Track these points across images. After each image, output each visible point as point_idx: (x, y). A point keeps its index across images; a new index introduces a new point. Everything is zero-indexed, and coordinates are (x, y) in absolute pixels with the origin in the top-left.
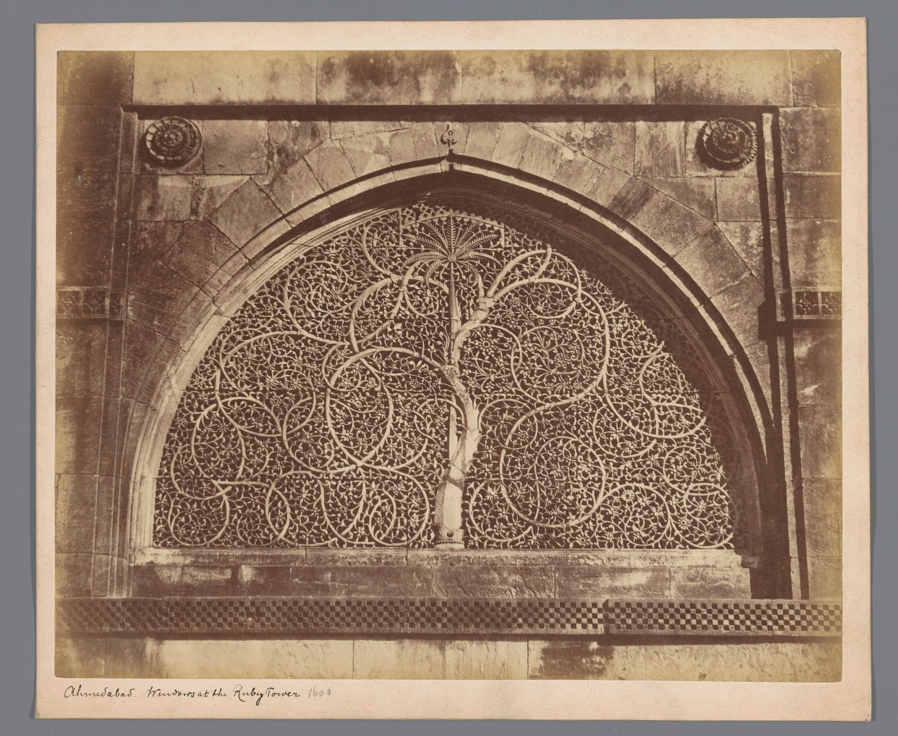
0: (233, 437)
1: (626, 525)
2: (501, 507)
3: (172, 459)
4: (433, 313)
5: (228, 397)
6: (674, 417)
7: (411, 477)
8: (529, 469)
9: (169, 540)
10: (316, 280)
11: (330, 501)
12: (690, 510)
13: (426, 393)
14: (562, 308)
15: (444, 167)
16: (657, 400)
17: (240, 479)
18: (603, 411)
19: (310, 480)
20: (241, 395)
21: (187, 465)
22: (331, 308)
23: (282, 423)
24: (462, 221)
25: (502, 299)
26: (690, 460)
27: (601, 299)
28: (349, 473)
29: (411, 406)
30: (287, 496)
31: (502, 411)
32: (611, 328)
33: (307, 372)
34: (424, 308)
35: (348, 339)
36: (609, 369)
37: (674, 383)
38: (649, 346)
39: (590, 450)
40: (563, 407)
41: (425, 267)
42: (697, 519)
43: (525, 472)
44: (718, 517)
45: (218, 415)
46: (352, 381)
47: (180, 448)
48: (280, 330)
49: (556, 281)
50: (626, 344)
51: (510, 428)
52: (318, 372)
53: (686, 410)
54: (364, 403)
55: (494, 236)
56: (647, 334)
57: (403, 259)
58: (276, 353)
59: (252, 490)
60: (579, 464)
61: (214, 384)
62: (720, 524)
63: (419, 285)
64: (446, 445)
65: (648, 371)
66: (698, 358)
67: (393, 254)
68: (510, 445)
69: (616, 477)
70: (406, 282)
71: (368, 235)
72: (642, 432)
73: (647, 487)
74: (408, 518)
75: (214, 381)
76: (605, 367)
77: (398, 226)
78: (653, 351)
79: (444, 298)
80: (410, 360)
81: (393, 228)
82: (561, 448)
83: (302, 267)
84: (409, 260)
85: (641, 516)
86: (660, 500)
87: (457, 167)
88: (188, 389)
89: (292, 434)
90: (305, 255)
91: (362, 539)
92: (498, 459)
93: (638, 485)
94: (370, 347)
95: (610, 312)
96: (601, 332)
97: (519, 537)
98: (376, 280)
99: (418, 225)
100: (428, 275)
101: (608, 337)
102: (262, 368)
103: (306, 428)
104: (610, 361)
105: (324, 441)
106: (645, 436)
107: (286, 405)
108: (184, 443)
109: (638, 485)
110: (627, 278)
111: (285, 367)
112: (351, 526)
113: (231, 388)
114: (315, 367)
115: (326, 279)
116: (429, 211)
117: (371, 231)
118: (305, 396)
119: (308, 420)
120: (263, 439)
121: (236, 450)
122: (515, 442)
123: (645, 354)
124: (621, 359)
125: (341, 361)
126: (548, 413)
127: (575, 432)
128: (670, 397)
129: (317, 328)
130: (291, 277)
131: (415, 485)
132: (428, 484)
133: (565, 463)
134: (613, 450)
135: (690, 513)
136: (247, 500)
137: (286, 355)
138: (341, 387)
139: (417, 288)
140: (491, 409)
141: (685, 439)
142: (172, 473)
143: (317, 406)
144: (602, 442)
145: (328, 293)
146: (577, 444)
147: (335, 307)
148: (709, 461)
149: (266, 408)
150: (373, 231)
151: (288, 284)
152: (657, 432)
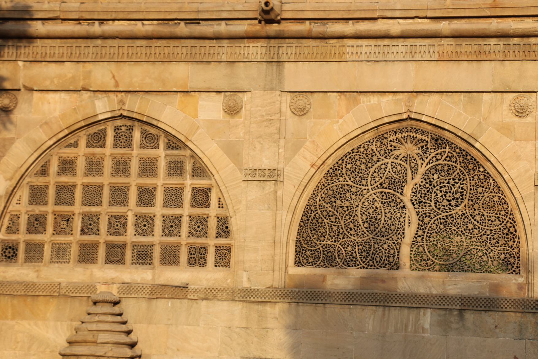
3: (301, 232)
4: (400, 176)
6: (493, 220)
7: (390, 242)
9: (301, 264)
10: (356, 161)
11: (360, 251)
13: (397, 208)
14: (452, 174)
15: (405, 116)
16: (487, 213)
17: (326, 241)
18: (466, 217)
19: (352, 242)
20: (327, 208)
22: (361, 173)
23: (342, 219)
24: (413, 137)
25: (428, 170)
27: (467, 170)
28: (367, 240)
29: (391, 213)
30: (344, 248)
31: (426, 216)
32: (470, 183)
34: (397, 173)
35: (367, 186)
36: (469, 200)
37: (494, 206)
38: (485, 191)
39: (460, 233)
40: (450, 215)
41: (398, 156)
42: (501, 262)
44: (509, 261)
47: (304, 229)
49: (450, 163)
50: (476, 190)
51: (429, 223)
52: (356, 199)
53: (499, 217)
54: (373, 212)
55: (426, 143)
57: (389, 153)
59: (331, 246)
62: (510, 264)
63: (395, 164)
64: (404, 230)
66: (505, 196)
67: (385, 151)
68: (429, 230)
70: (390, 163)
71: (376, 142)
72: (480, 226)
74: (389, 258)
75: (316, 202)
76: (467, 199)
78: (487, 193)
79: (405, 169)
82: (448, 232)
83: (350, 156)
84: (392, 153)
89: (346, 224)
90: (352, 150)
91: (371, 266)
92: (423, 235)
93: (478, 247)
94: (375, 189)
95: (471, 176)
97: (431, 267)
98: (378, 161)
100: (399, 159)
102: (335, 197)
103: (351, 222)
104: (469, 197)
105: (358, 227)
106: (482, 228)
107: (344, 212)
108: (306, 227)
109: (478, 247)
110: (478, 162)
111: (343, 197)
112: (367, 261)
114: (355, 198)
115: (359, 161)
116: (400, 132)
118: (351, 209)
119: (352, 218)
120: (335, 226)
121: (325, 230)
122: (430, 229)
123: (483, 194)
124: (474, 196)
127: (454, 226)
128: (493, 212)
129: (355, 181)
130: (345, 160)
131: (392, 245)
132: (397, 245)
133: (450, 238)
134: (469, 233)
135: (498, 259)
136: (329, 250)
137: (343, 192)
138: (365, 205)
139: (395, 165)
140: (422, 215)
141: (498, 229)
142: (301, 238)
144: (465, 230)
145: (360, 167)
146: (455, 230)
148: (507, 238)
149: (335, 213)
151: (345, 163)
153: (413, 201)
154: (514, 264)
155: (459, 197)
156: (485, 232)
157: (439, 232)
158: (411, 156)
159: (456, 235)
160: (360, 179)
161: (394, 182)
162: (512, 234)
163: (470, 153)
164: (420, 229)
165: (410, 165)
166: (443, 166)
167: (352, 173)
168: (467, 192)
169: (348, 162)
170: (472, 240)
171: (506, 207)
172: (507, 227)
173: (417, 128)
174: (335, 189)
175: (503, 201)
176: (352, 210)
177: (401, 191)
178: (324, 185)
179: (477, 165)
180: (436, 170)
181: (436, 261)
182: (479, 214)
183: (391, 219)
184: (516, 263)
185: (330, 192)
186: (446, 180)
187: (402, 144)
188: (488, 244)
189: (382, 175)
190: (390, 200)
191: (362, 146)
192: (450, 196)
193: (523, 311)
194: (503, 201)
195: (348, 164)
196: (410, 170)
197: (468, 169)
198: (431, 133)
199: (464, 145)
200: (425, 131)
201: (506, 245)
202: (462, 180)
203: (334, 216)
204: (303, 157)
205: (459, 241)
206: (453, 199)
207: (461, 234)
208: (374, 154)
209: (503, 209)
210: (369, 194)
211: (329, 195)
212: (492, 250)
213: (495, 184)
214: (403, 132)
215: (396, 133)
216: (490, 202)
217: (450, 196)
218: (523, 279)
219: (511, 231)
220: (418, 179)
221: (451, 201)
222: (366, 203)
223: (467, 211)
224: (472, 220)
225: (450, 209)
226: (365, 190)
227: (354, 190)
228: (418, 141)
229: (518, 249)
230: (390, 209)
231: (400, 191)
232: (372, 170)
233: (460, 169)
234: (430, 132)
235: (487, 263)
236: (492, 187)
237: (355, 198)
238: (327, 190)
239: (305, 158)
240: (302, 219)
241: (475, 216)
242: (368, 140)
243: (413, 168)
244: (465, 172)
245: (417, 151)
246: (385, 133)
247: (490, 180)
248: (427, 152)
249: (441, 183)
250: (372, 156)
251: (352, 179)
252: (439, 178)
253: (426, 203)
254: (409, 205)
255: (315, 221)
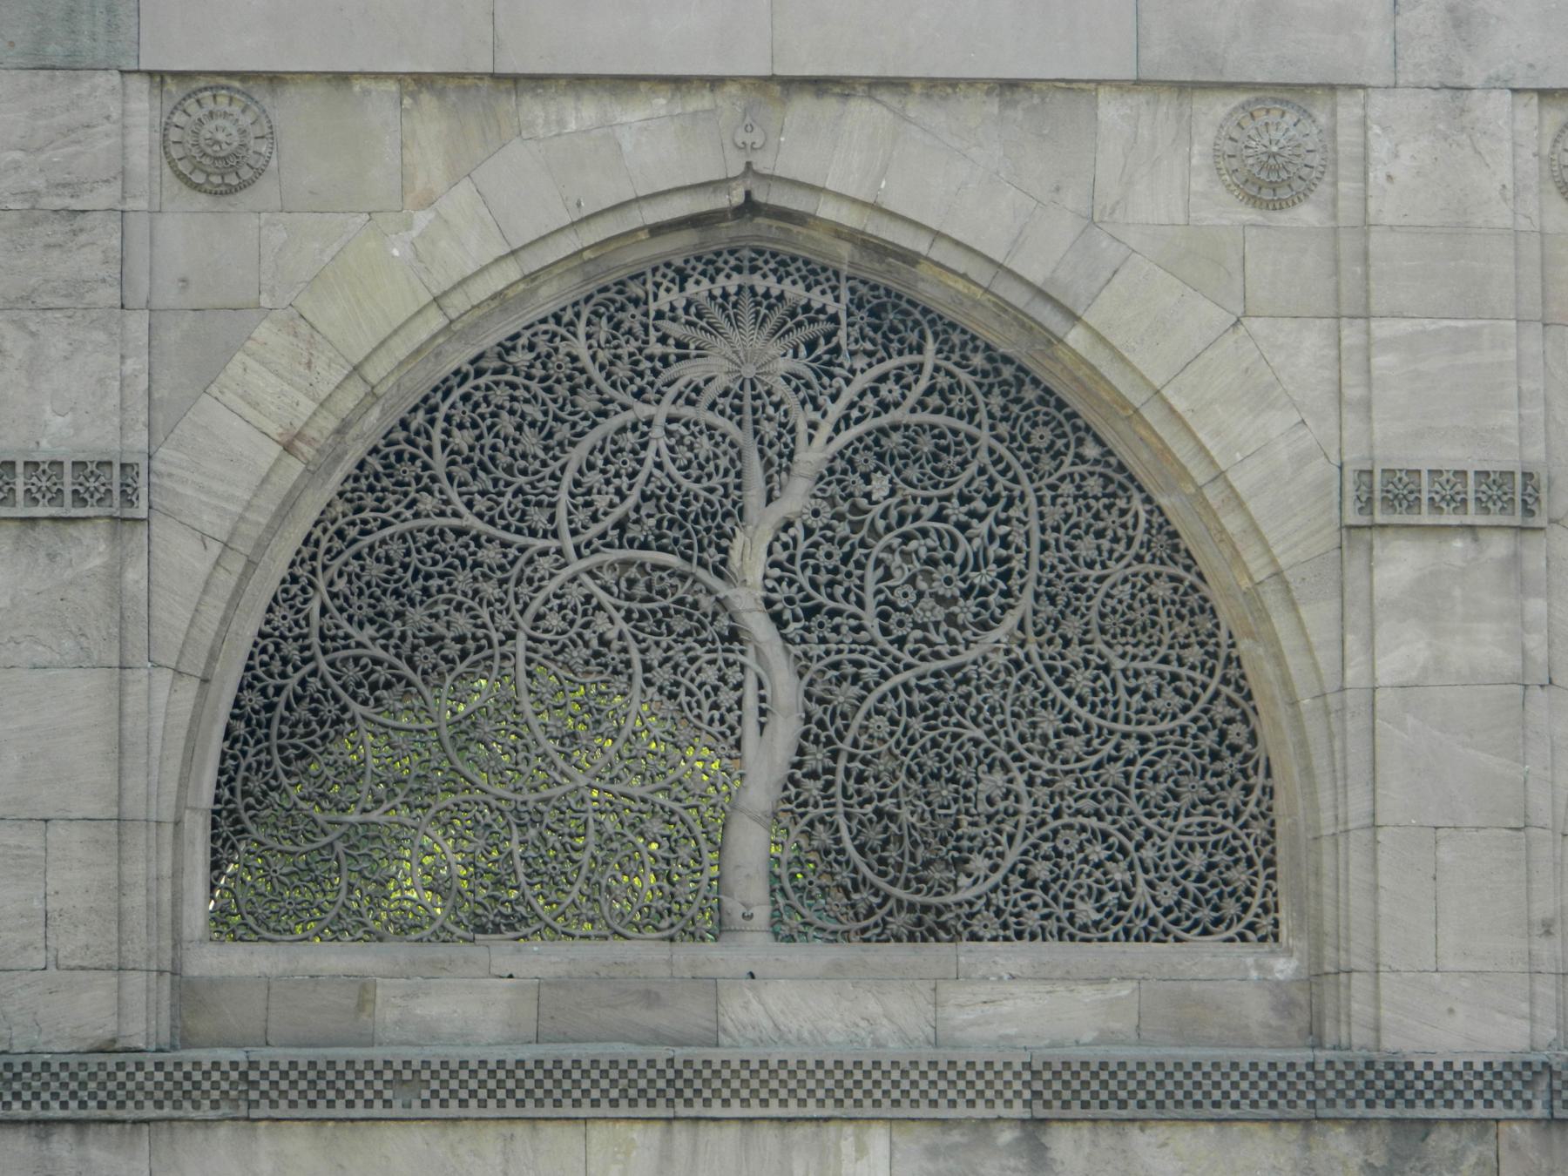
0: (348, 726)
1: (1063, 897)
2: (839, 863)
4: (712, 483)
5: (336, 649)
6: (1153, 690)
8: (889, 790)
10: (493, 415)
12: (1178, 867)
13: (702, 643)
14: (953, 474)
16: (1123, 656)
18: (1025, 679)
20: (359, 645)
21: (267, 783)
22: (524, 472)
24: (767, 295)
25: (841, 454)
26: (1181, 774)
27: (1025, 456)
29: (675, 667)
31: (840, 680)
32: (1042, 516)
33: (481, 600)
34: (694, 472)
35: (555, 534)
36: (1037, 596)
37: (1154, 624)
38: (1111, 551)
39: (1000, 753)
40: (952, 671)
41: (697, 390)
42: (1191, 886)
43: (881, 797)
44: (1226, 883)
45: (319, 686)
46: (564, 618)
47: (251, 751)
48: (428, 516)
50: (1070, 547)
52: (501, 601)
53: (1175, 677)
54: (587, 663)
55: (830, 326)
56: (1105, 529)
57: (655, 373)
58: (422, 562)
60: (979, 780)
61: (308, 625)
62: (1231, 894)
63: (686, 425)
65: (1109, 601)
66: (1200, 575)
67: (636, 363)
68: (855, 744)
69: (1045, 806)
70: (660, 420)
71: (589, 323)
72: (1094, 720)
73: (1103, 825)
75: (307, 618)
77: (646, 303)
78: (1118, 560)
79: (733, 453)
80: (671, 575)
81: (636, 305)
82: (948, 750)
83: (466, 388)
84: (667, 374)
85: (1090, 881)
86: (1122, 850)
87: (760, 197)
88: (262, 635)
90: (472, 362)
92: (831, 771)
93: (1085, 821)
94: (594, 552)
96: (1025, 523)
97: (871, 921)
98: (605, 414)
99: (684, 303)
100: (705, 400)
101: (1036, 537)
102: (397, 594)
104: (1039, 582)
106: (1100, 728)
107: (444, 666)
108: (258, 742)
109: (1085, 821)
110: (1074, 415)
111: (440, 590)
113: (341, 633)
114: (498, 593)
115: (512, 412)
116: (703, 273)
117: (596, 313)
118: (479, 649)
123: (1104, 566)
124: (1059, 576)
125: (542, 579)
126: (923, 683)
127: (974, 720)
128: (1148, 652)
129: (496, 512)
130: (444, 408)
133: (953, 780)
134: (1042, 754)
135: (1178, 874)
137: (440, 568)
139: (683, 431)
141: (1172, 732)
142: (238, 799)
143: (501, 668)
144: (1022, 739)
145: (516, 442)
146: (977, 743)
147: (531, 469)
148: (1216, 774)
149: (406, 670)
150: (596, 313)
152: (1122, 718)
153: (778, 607)
154: (1249, 893)
155: (993, 584)
156: (1118, 748)
157: (905, 753)
158: (760, 388)
159: (984, 767)
160: (518, 502)
161: (684, 515)
162: (1239, 756)
163: (1039, 373)
164: (817, 741)
165: (756, 432)
166: (912, 433)
167: (481, 473)
168: (1027, 558)
169: (457, 419)
170: (1056, 788)
171: (1209, 625)
172: (1212, 720)
173: (786, 249)
174: (396, 549)
175: (1193, 600)
176: (487, 652)
177: (718, 557)
178: (340, 534)
179: (1067, 428)
180: (881, 457)
181: (898, 892)
182: (1087, 663)
183: (673, 696)
184: (1258, 890)
185: (376, 570)
186: (927, 501)
187: (713, 329)
188: (1132, 804)
189: (624, 483)
190: (668, 602)
191: (523, 341)
192: (948, 581)
193: (1310, 1113)
194: (1193, 600)
195: (455, 431)
196: (756, 456)
197: (1031, 450)
198: (848, 279)
199: (1006, 341)
200: (824, 269)
201: (1214, 807)
202: (1002, 502)
203: (400, 687)
204: (241, 397)
205: (997, 794)
206: (966, 594)
207: (1007, 758)
208: (581, 379)
209: (1193, 639)
210: (565, 573)
211: (369, 584)
212: (1148, 834)
213: (1157, 519)
214: (718, 271)
215: (682, 278)
216: (1137, 605)
217: (948, 581)
218: (1294, 963)
219: (1232, 738)
220: (796, 498)
221: (954, 600)
222: (554, 621)
223: (1032, 648)
224: (1057, 691)
225: (952, 641)
226: (544, 553)
227: (491, 555)
228: (793, 315)
229: (1264, 823)
230: (669, 648)
231: (712, 556)
232: (576, 456)
233: (991, 451)
234: (845, 270)
235: (1130, 895)
236: (1140, 536)
237: (498, 593)
238: (358, 556)
239: (255, 405)
240: (237, 704)
241: (1066, 673)
242: (551, 308)
243: (771, 445)
244: (1016, 465)
245: (784, 365)
246: (632, 278)
247: (1129, 499)
248: (837, 370)
249: (902, 520)
250: (573, 391)
251: (481, 504)
252: (892, 493)
253: (839, 613)
254: (759, 626)
255: (302, 712)
